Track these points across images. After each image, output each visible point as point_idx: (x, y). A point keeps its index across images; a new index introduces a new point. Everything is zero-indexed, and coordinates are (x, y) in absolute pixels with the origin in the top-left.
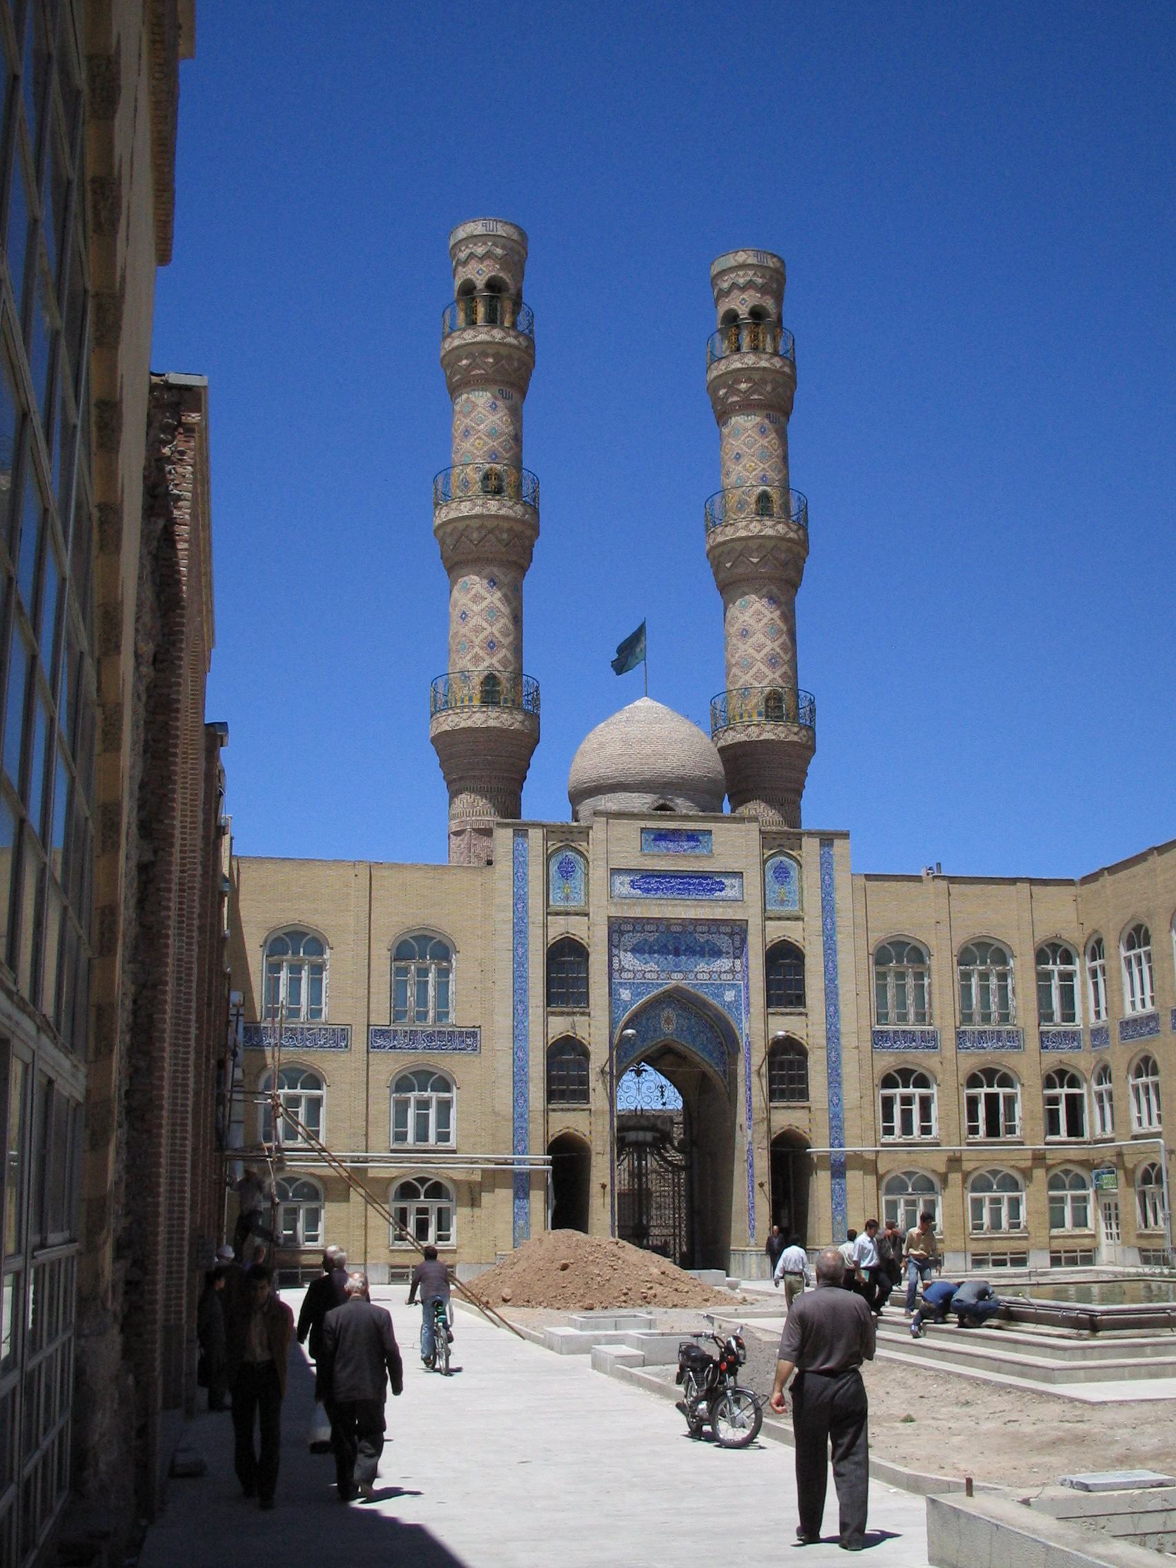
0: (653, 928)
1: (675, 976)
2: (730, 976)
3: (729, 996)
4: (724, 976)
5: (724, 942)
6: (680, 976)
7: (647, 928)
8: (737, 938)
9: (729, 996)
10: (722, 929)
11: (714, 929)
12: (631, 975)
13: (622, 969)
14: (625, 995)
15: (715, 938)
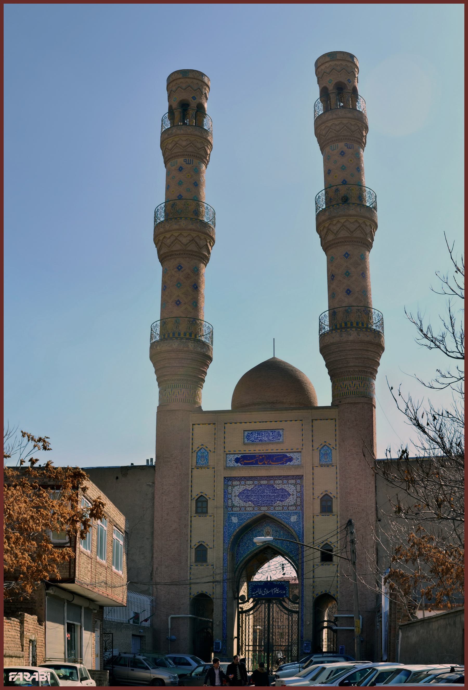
0: (251, 482)
1: (262, 508)
2: (294, 508)
3: (293, 519)
4: (290, 508)
5: (291, 489)
6: (266, 508)
7: (248, 482)
8: (298, 486)
9: (293, 519)
10: (291, 481)
11: (285, 481)
12: (238, 509)
13: (233, 506)
14: (235, 520)
15: (286, 487)
